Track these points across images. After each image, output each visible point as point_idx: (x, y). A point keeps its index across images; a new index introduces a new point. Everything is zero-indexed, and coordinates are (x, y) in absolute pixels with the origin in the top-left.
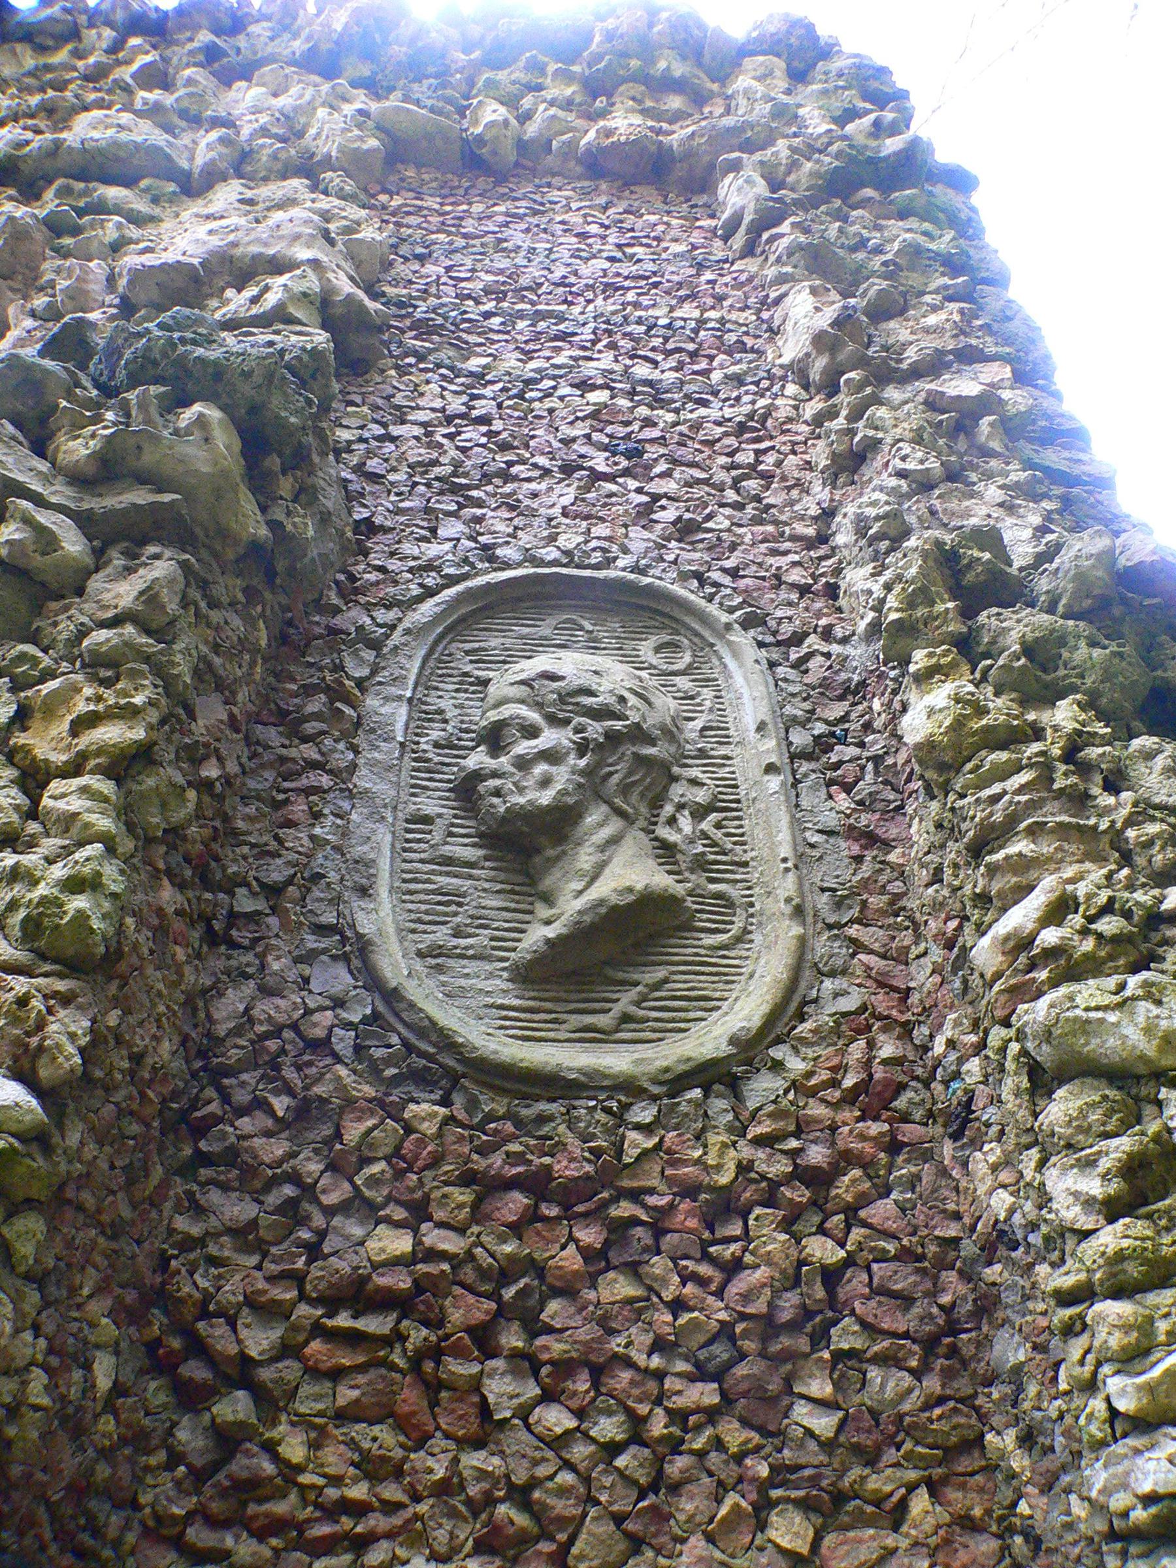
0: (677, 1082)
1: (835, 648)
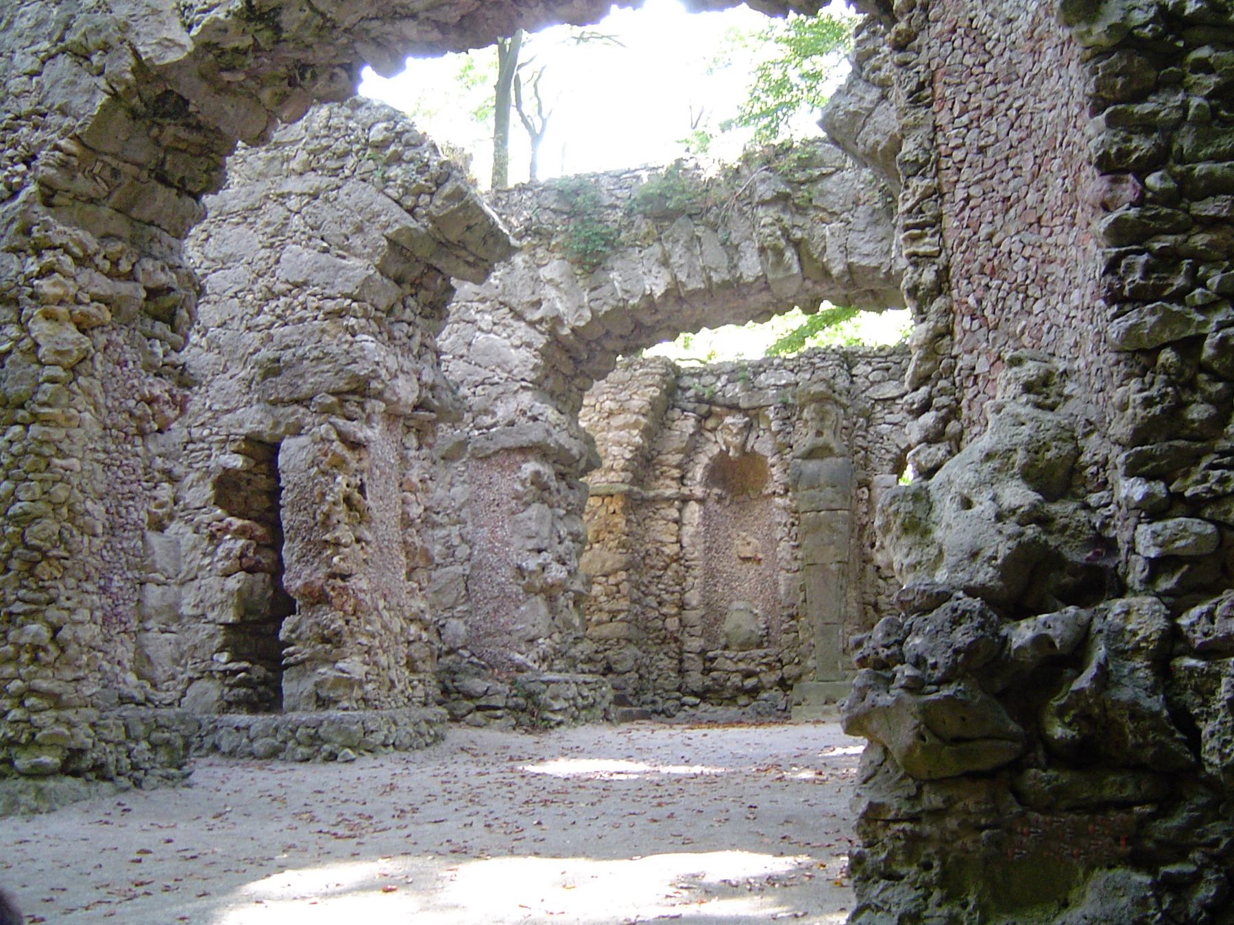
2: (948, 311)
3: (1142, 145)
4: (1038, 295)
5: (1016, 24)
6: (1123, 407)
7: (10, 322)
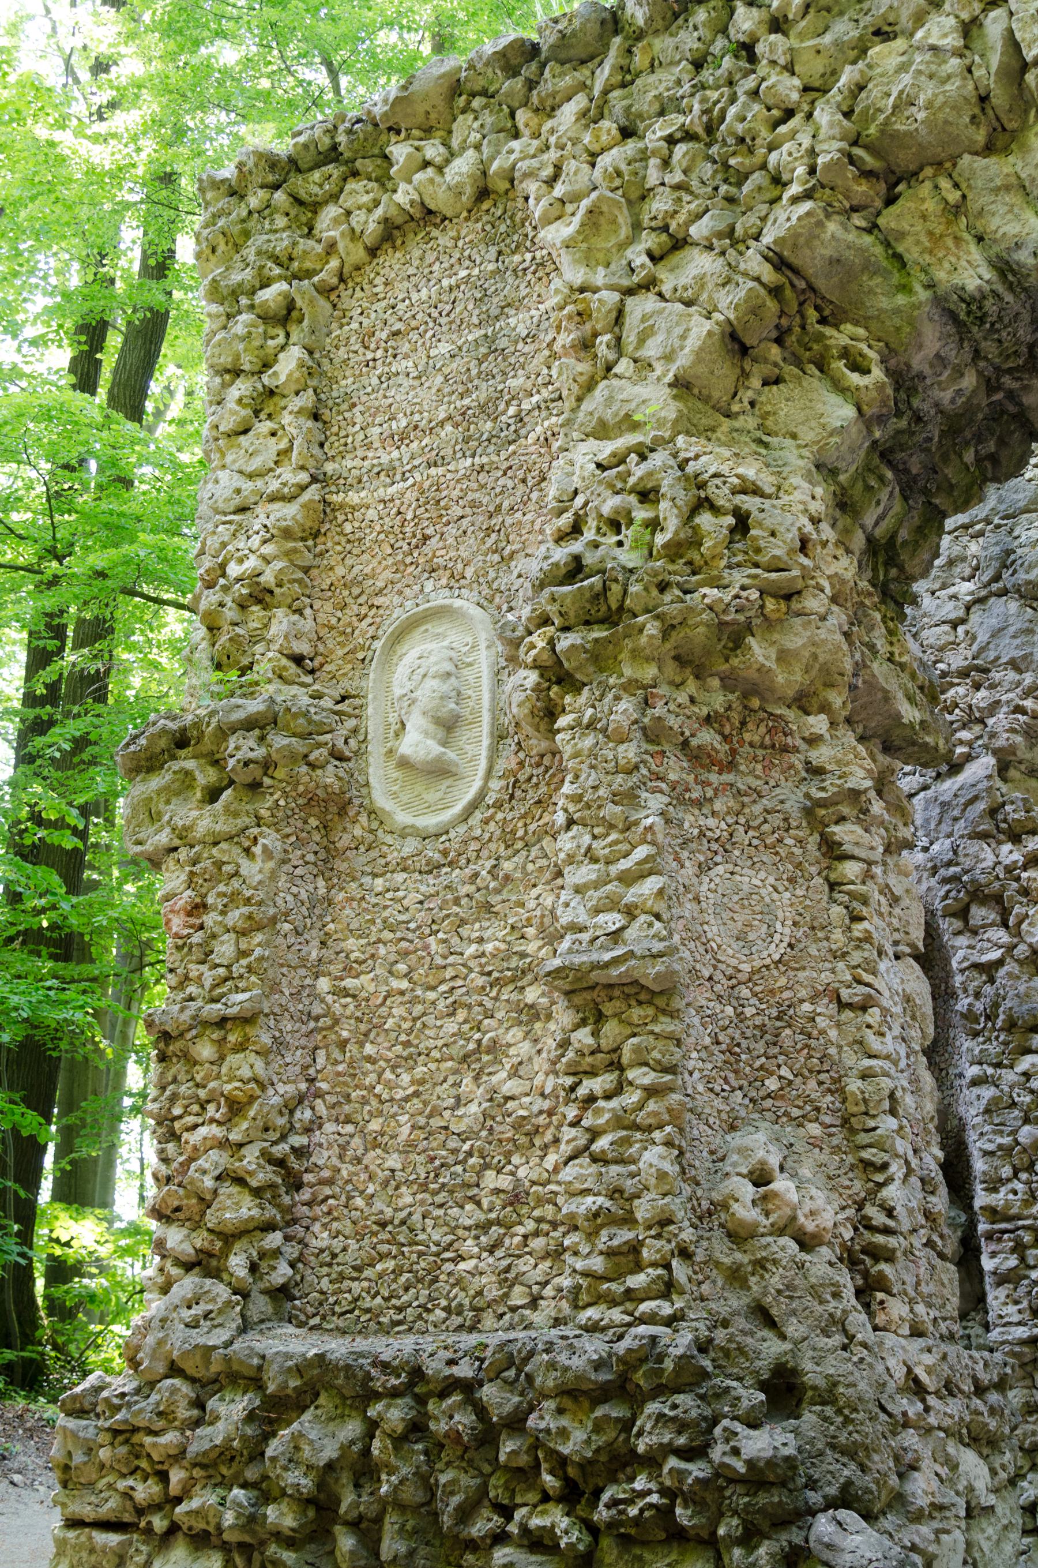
7: (991, 925)
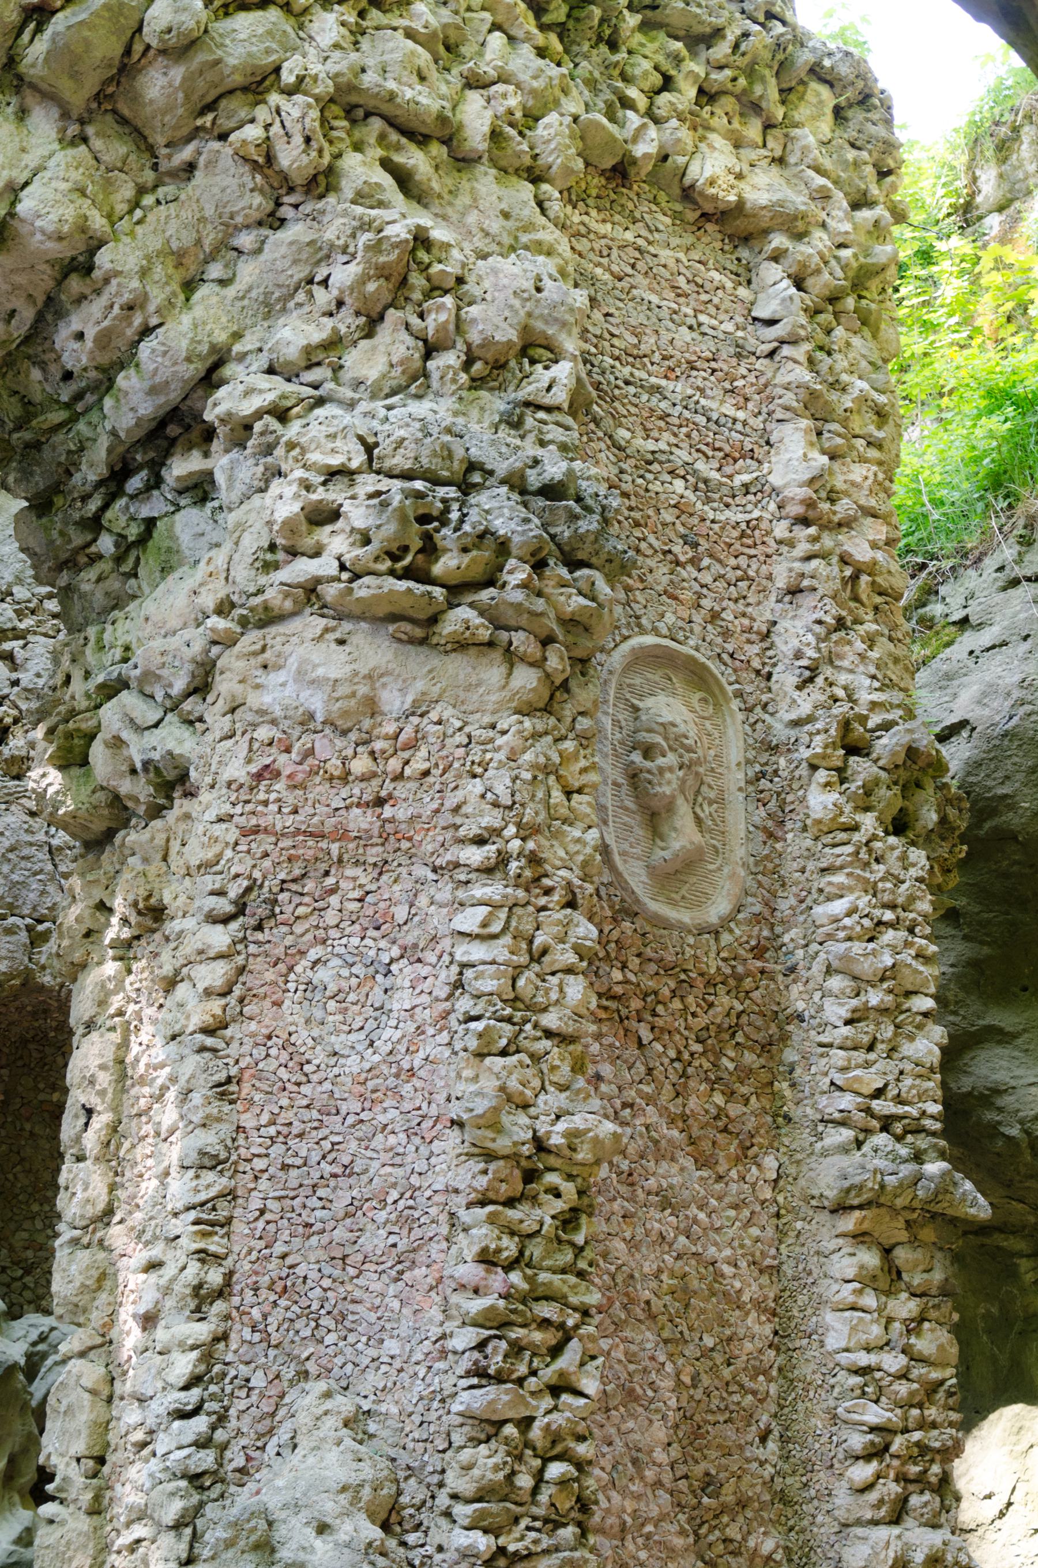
0: (702, 931)
1: (767, 717)
2: (228, 1317)
3: (510, 1247)
4: (332, 1327)
5: (342, 1061)
6: (468, 1468)
